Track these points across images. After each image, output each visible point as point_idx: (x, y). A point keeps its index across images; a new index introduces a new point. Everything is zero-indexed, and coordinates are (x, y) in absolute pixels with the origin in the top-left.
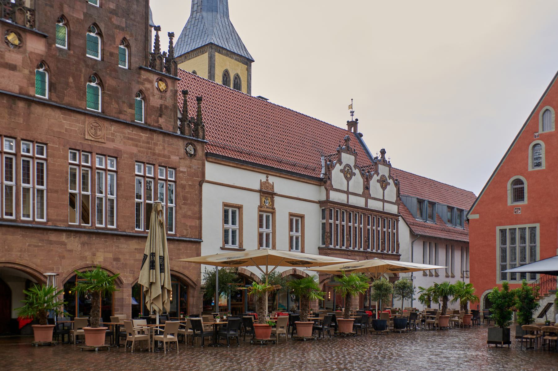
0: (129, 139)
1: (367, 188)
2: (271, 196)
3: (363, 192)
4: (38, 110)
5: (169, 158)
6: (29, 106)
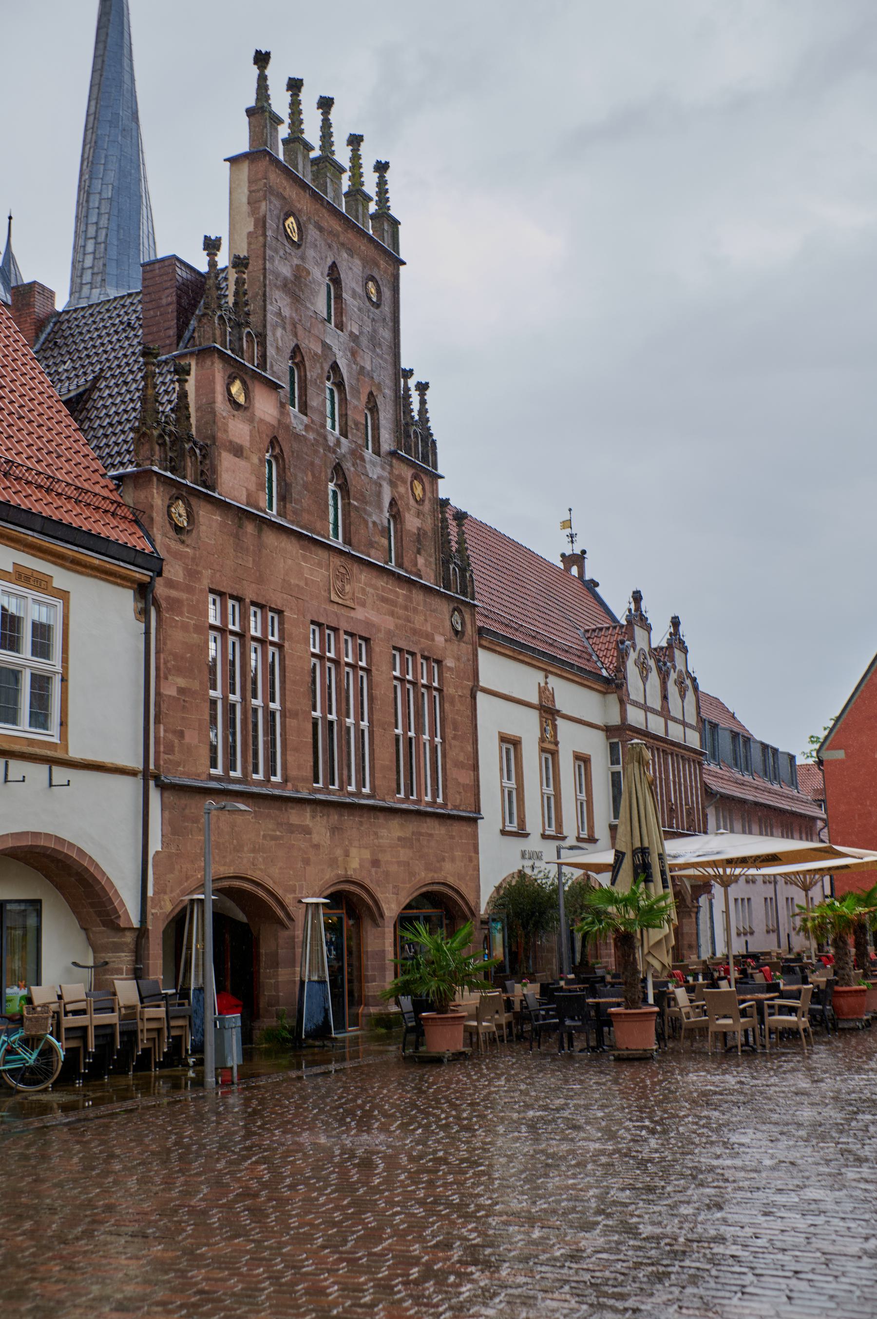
0: (384, 600)
1: (665, 698)
2: (550, 717)
3: (662, 708)
4: (271, 539)
5: (433, 640)
6: (260, 531)
